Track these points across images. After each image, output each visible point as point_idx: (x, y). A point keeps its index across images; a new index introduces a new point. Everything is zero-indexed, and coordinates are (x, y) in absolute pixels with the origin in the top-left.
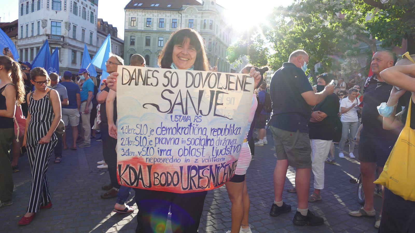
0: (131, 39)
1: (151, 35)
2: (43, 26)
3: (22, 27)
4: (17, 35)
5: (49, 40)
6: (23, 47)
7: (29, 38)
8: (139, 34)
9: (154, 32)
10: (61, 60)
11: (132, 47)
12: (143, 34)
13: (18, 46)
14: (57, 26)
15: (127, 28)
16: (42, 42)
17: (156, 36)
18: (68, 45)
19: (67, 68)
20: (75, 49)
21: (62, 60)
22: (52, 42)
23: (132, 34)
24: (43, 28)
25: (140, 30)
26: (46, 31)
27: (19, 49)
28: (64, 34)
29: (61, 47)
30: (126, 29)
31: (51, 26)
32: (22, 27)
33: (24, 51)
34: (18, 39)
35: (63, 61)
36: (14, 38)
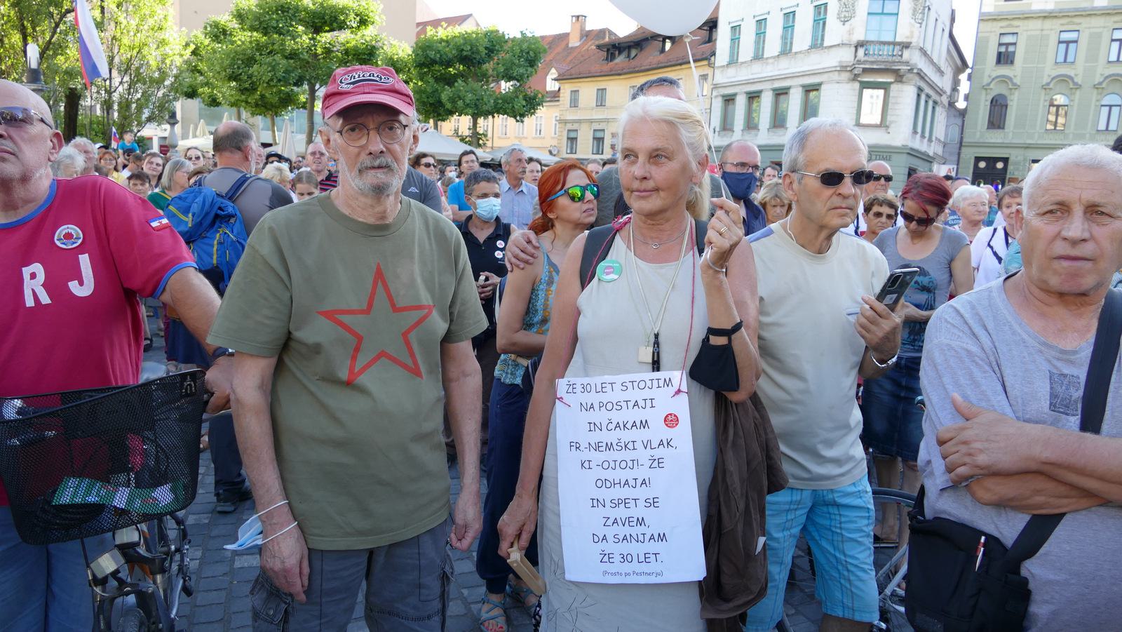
0: (1000, 45)
1: (1080, 24)
2: (845, 17)
3: (735, 29)
4: (714, 54)
5: (866, 58)
6: (740, 87)
7: (770, 61)
8: (1038, 24)
9: (1095, 14)
10: (888, 123)
11: (1004, 70)
12: (1048, 24)
13: (716, 87)
14: (885, 12)
15: (989, 8)
16: (838, 69)
17: (991, 32)
18: (915, 71)
19: (905, 147)
20: (923, 85)
21: (891, 122)
22: (875, 67)
23: (1008, 26)
24: (844, 22)
25: (1042, 11)
26: (850, 33)
27: (716, 97)
28: (907, 37)
29: (893, 80)
30: (983, 11)
31: (883, 16)
32: (735, 29)
33: (741, 102)
34: (716, 65)
35: (892, 125)
36: (705, 62)
